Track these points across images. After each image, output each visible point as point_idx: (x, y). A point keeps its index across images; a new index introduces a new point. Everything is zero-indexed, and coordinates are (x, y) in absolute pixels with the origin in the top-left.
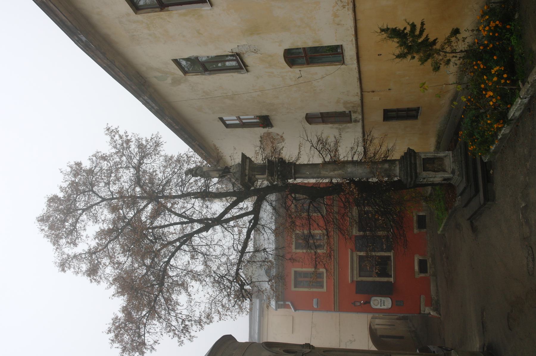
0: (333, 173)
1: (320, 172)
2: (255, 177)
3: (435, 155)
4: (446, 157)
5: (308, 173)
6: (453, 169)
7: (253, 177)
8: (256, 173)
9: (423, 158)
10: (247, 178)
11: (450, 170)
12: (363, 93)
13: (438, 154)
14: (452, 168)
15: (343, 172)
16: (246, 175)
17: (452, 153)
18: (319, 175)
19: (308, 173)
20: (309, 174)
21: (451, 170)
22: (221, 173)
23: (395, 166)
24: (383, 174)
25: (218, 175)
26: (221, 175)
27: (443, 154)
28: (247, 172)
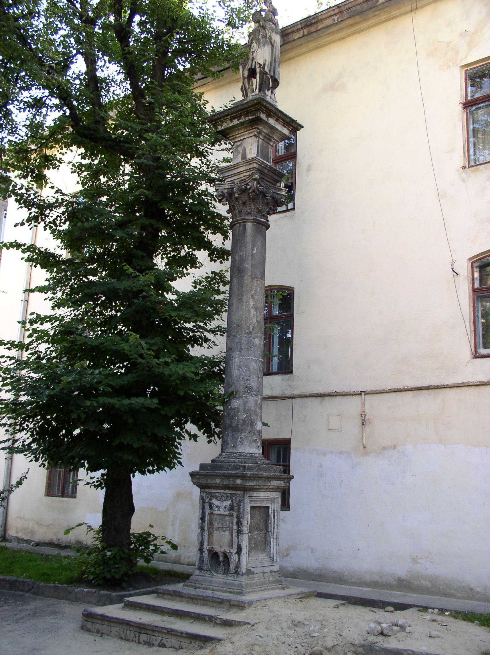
0: (252, 305)
1: (256, 278)
2: (255, 135)
3: (275, 534)
4: (270, 557)
5: (254, 252)
6: (253, 573)
7: (255, 132)
8: (260, 141)
9: (268, 507)
10: (263, 116)
11: (251, 565)
12: (363, 394)
13: (275, 542)
14: (256, 570)
15: (253, 329)
16: (269, 116)
17: (276, 570)
18: (249, 274)
19: (254, 252)
20: (253, 254)
21: (252, 570)
22: (267, 69)
23: (259, 444)
24: (245, 416)
25: (262, 64)
26: (258, 70)
27: (275, 553)
28: (272, 121)
